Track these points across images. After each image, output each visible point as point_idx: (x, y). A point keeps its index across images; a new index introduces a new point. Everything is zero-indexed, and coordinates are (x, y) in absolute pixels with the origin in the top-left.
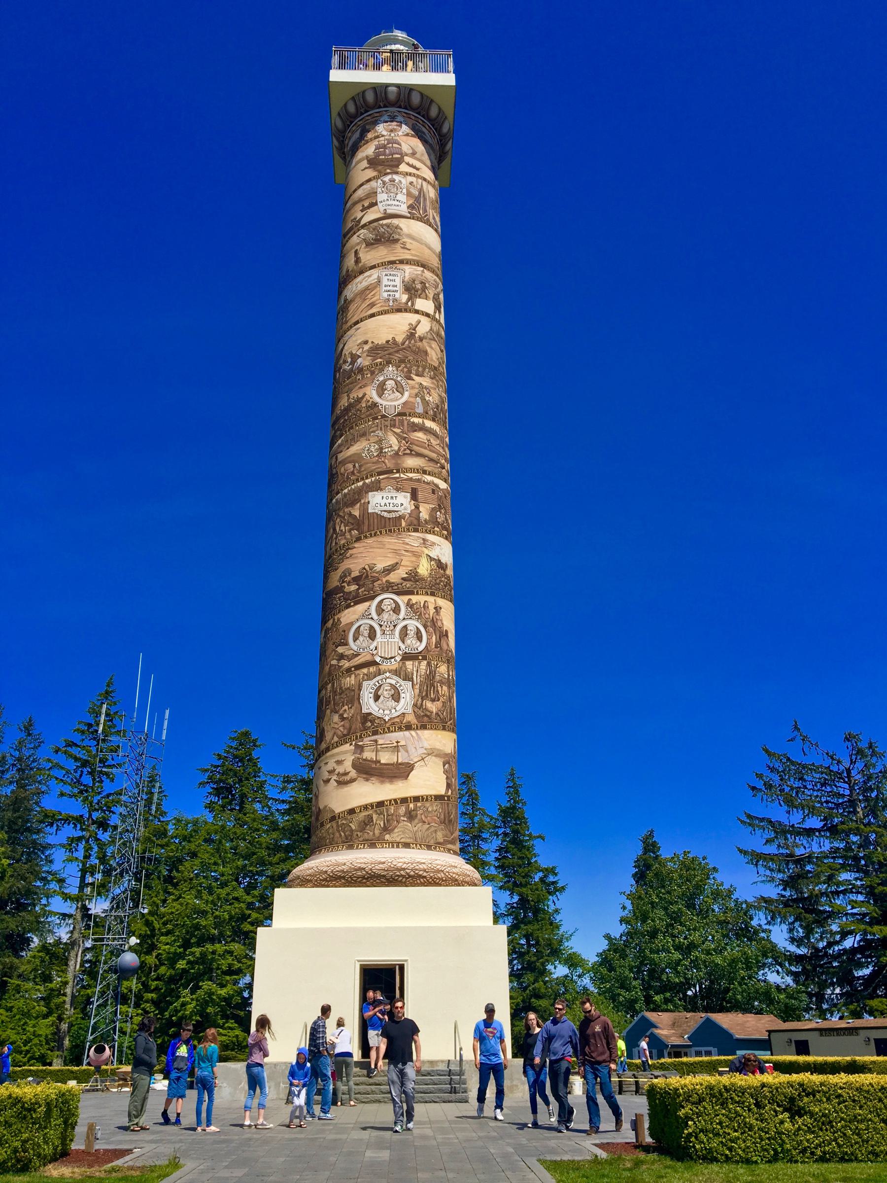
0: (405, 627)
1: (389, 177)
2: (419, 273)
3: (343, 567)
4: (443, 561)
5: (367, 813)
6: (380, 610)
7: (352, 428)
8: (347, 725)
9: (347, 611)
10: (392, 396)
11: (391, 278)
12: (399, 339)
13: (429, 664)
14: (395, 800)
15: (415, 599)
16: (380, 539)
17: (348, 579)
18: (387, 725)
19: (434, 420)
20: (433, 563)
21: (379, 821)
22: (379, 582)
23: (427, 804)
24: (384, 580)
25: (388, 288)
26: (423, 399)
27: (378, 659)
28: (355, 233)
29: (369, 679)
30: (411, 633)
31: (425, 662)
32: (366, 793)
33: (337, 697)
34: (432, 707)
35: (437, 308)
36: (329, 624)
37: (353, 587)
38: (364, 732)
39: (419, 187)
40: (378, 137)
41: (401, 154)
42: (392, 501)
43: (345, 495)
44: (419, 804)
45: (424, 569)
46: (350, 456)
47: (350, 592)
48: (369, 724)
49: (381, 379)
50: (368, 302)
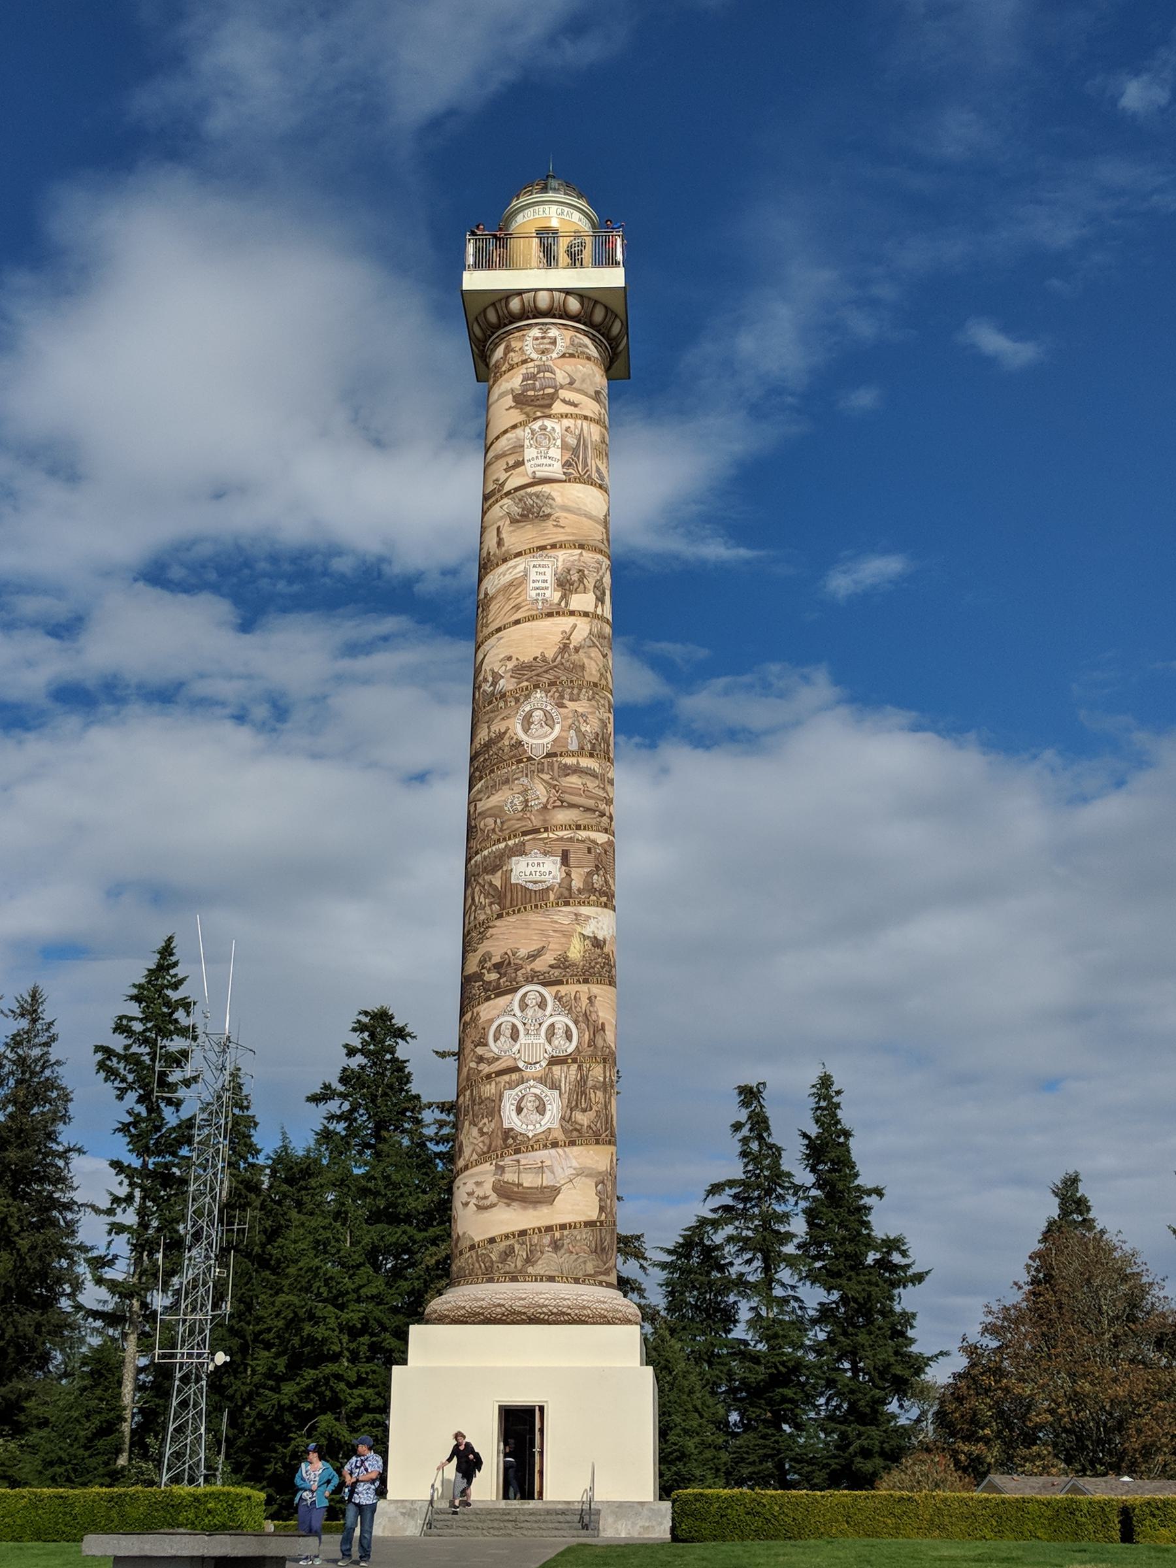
0: (552, 1025)
1: (539, 423)
2: (576, 558)
3: (482, 949)
4: (600, 937)
5: (508, 1243)
6: (523, 1006)
7: (492, 771)
8: (487, 1142)
9: (487, 1004)
10: (541, 732)
11: (541, 570)
12: (550, 655)
13: (580, 1068)
14: (539, 1229)
15: (563, 989)
16: (523, 916)
17: (488, 965)
18: (531, 1143)
19: (591, 755)
20: (587, 942)
21: (521, 1252)
22: (523, 971)
23: (575, 1232)
24: (529, 968)
25: (536, 585)
26: (578, 731)
27: (521, 1065)
28: (497, 501)
30: (560, 1031)
31: (576, 1065)
32: (509, 1219)
33: (476, 1108)
34: (583, 1119)
35: (600, 600)
36: (468, 1017)
37: (494, 976)
39: (577, 432)
40: (524, 362)
41: (555, 387)
42: (538, 869)
43: (485, 858)
44: (566, 1232)
45: (576, 951)
46: (491, 809)
49: (527, 709)
50: (512, 603)
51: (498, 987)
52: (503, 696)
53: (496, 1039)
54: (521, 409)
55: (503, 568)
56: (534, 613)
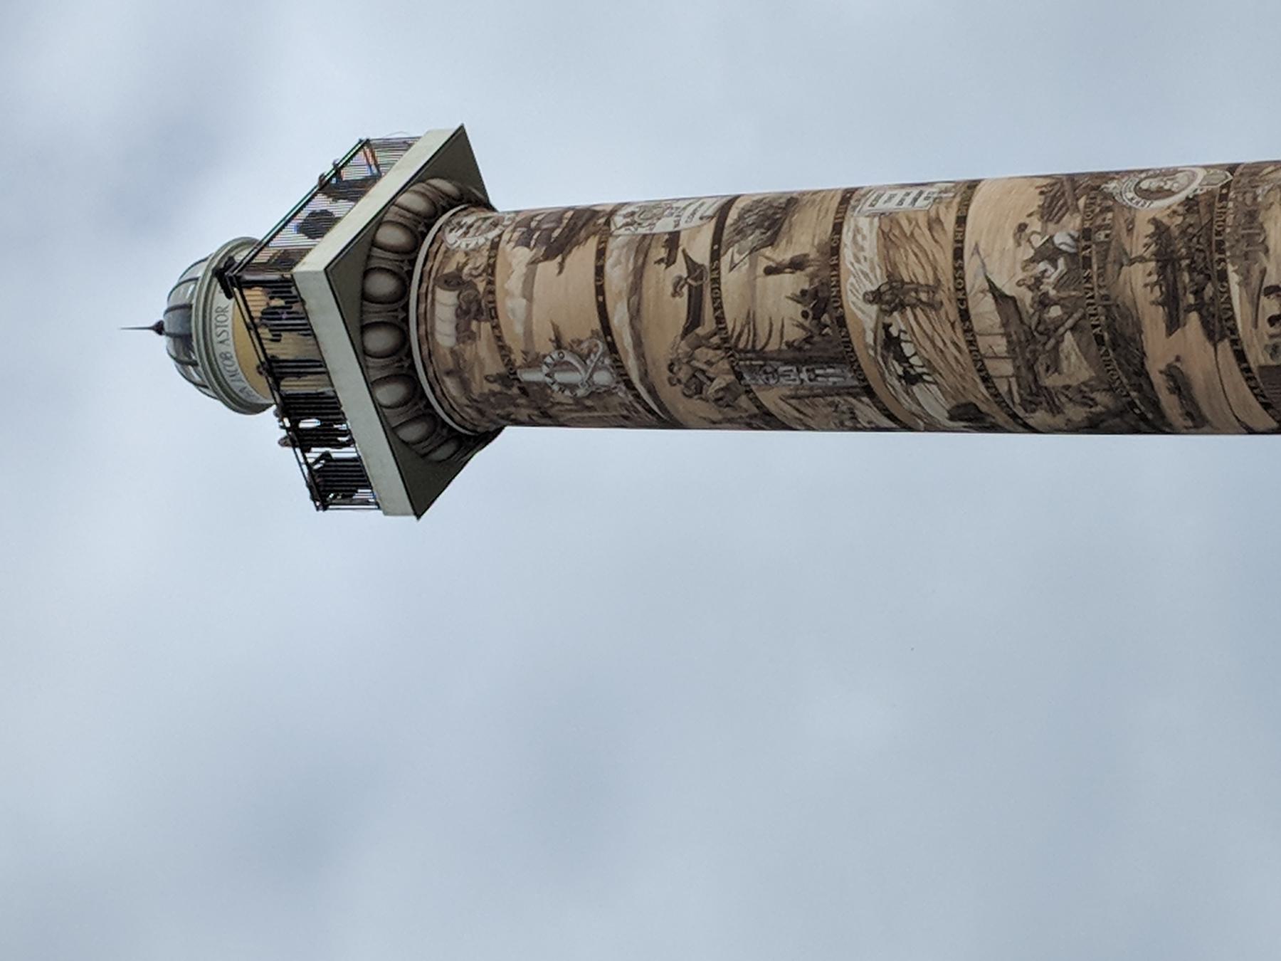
7: (1221, 243)
40: (495, 245)
52: (1086, 234)
54: (578, 243)
55: (847, 253)
56: (958, 199)
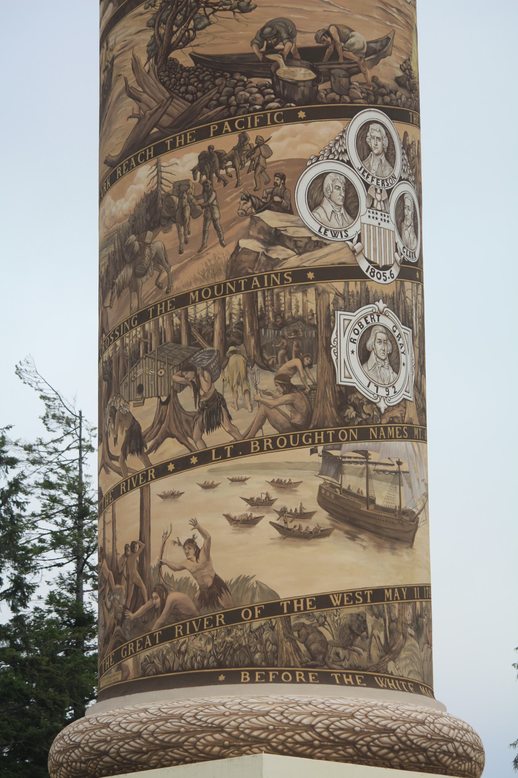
5: (354, 610)
6: (364, 150)
8: (302, 404)
9: (286, 128)
14: (399, 589)
17: (287, 47)
18: (384, 421)
27: (364, 265)
29: (350, 308)
33: (269, 333)
37: (302, 74)
38: (342, 429)
47: (296, 84)
48: (351, 412)
51: (313, 97)
53: (314, 205)
